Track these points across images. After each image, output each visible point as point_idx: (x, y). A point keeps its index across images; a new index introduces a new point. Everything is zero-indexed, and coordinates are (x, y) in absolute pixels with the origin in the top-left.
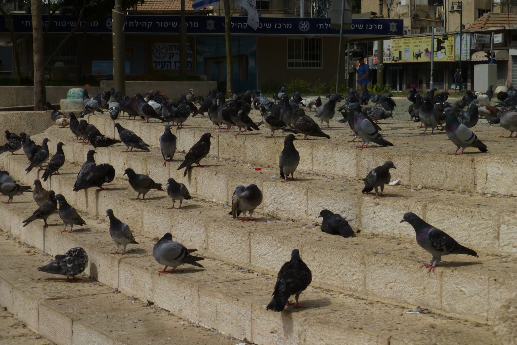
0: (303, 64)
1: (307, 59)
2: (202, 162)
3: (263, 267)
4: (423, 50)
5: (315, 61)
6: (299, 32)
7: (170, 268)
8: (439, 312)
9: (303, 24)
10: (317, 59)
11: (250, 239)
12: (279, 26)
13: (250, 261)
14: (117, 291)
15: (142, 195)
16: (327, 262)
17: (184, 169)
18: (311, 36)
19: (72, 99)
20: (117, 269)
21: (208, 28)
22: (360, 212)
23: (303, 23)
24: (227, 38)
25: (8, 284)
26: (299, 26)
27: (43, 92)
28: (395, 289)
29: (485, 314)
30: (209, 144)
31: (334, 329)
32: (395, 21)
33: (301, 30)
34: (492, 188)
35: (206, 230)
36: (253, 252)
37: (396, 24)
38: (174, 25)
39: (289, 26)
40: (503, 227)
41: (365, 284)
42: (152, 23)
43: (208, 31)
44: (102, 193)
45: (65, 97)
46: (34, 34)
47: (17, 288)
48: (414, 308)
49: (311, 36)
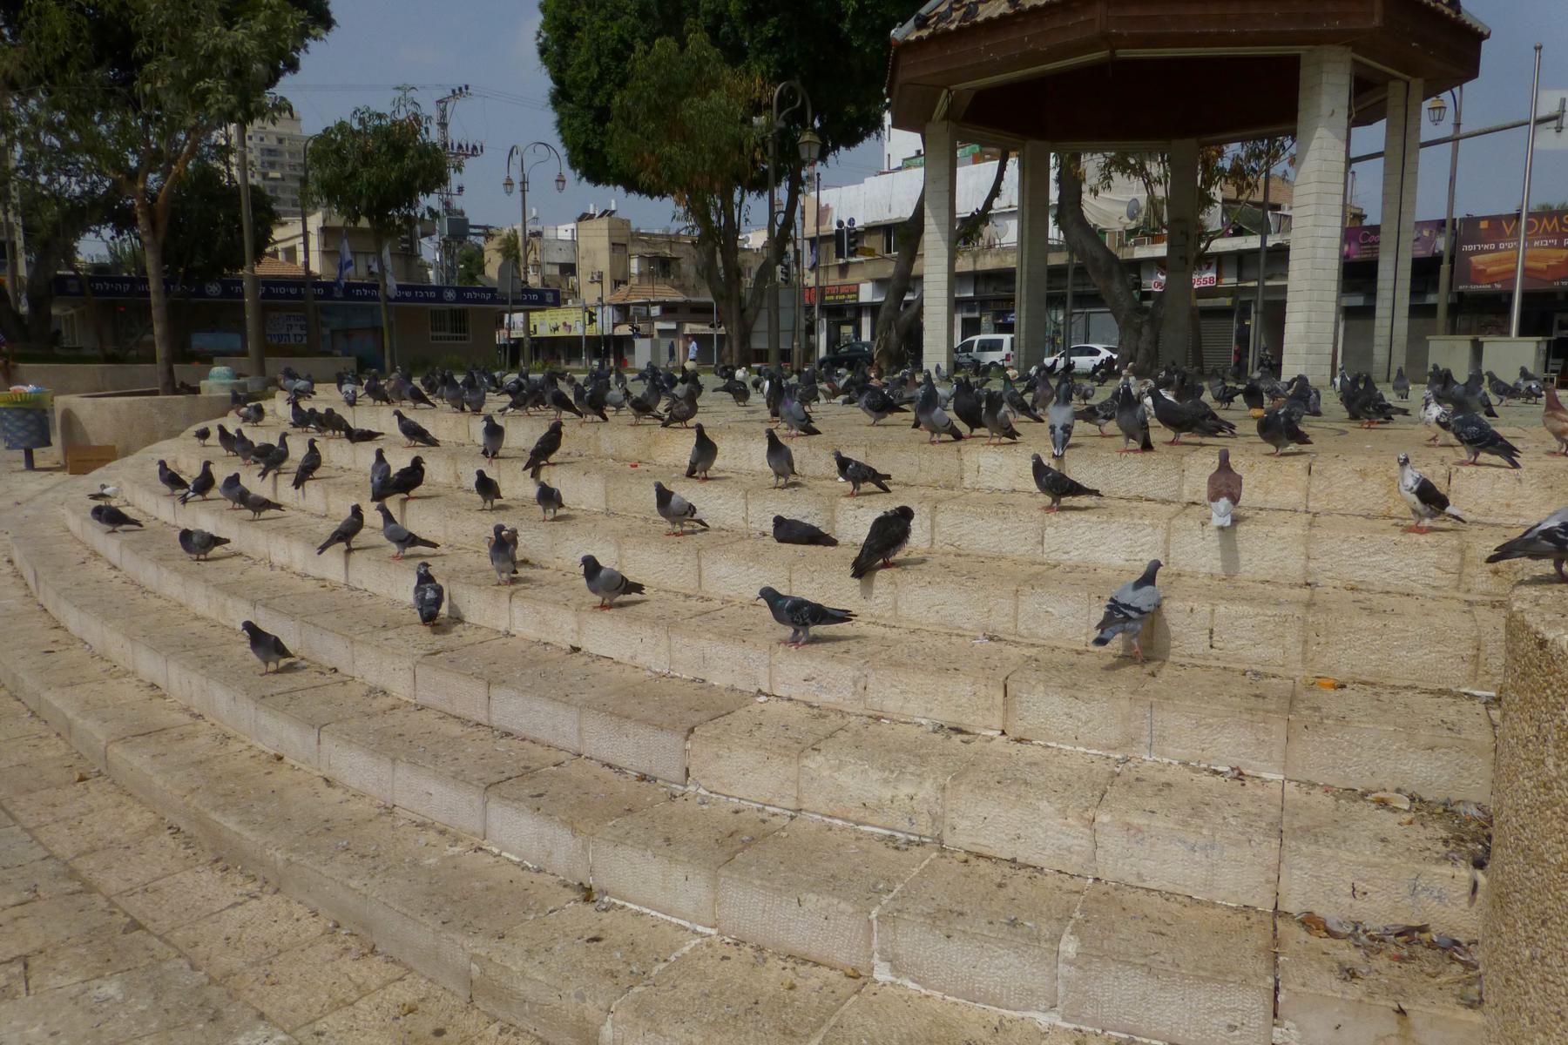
2: (553, 458)
3: (723, 592)
4: (560, 324)
6: (443, 301)
7: (606, 602)
8: (1012, 638)
11: (699, 558)
13: (700, 586)
14: (508, 634)
15: (489, 504)
16: (833, 583)
17: (530, 470)
19: (216, 381)
20: (506, 605)
21: (336, 295)
22: (833, 517)
27: (170, 372)
28: (942, 613)
29: (1083, 638)
30: (560, 434)
31: (914, 672)
32: (552, 291)
34: (986, 481)
35: (619, 547)
36: (704, 574)
38: (293, 291)
40: (1050, 531)
41: (895, 608)
43: (337, 299)
44: (411, 504)
45: (206, 377)
46: (154, 299)
47: (362, 642)
48: (980, 635)
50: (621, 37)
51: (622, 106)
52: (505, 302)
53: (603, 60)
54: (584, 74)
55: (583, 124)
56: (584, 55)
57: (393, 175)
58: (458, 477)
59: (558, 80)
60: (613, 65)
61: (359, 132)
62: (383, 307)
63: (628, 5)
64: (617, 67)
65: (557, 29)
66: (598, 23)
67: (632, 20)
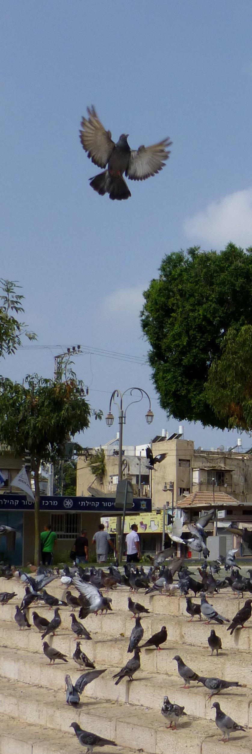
0: (64, 537)
1: (67, 532)
5: (75, 534)
9: (67, 502)
10: (76, 532)
12: (47, 503)
18: (73, 512)
23: (67, 501)
24: (36, 515)
25: (148, 729)
26: (64, 503)
32: (145, 500)
33: (66, 507)
37: (146, 502)
39: (56, 503)
42: (18, 501)
49: (73, 512)
50: (205, 317)
51: (216, 372)
52: (121, 509)
53: (191, 332)
54: (177, 342)
55: (174, 377)
56: (177, 328)
57: (53, 421)
58: (182, 637)
59: (155, 346)
60: (198, 336)
61: (28, 391)
62: (36, 515)
63: (210, 295)
64: (201, 337)
65: (157, 310)
66: (188, 307)
67: (213, 305)
